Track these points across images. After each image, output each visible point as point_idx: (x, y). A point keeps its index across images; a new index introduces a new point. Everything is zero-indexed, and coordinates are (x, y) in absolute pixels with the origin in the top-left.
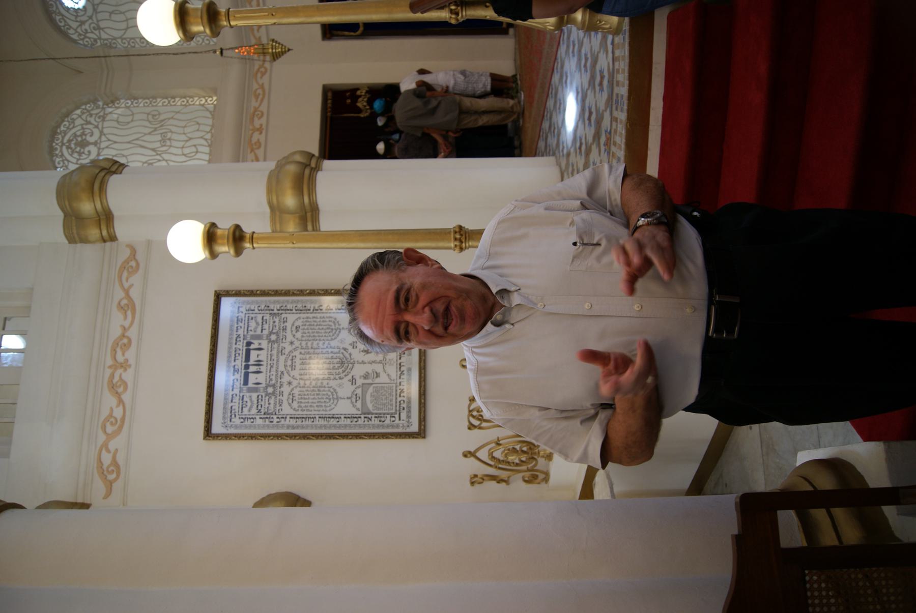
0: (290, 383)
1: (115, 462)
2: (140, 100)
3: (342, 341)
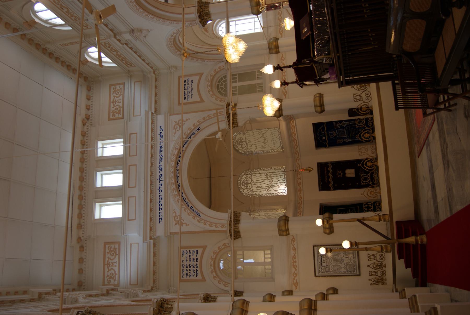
0: (331, 265)
1: (297, 282)
2: (262, 169)
3: (341, 256)
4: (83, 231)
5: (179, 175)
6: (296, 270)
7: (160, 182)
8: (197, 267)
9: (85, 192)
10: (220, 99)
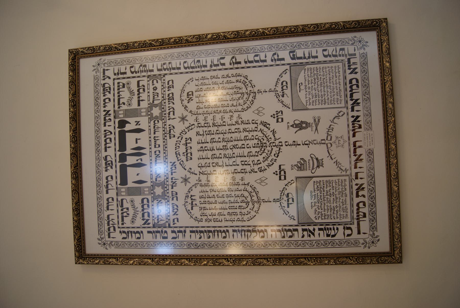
0: (186, 180)
3: (259, 112)
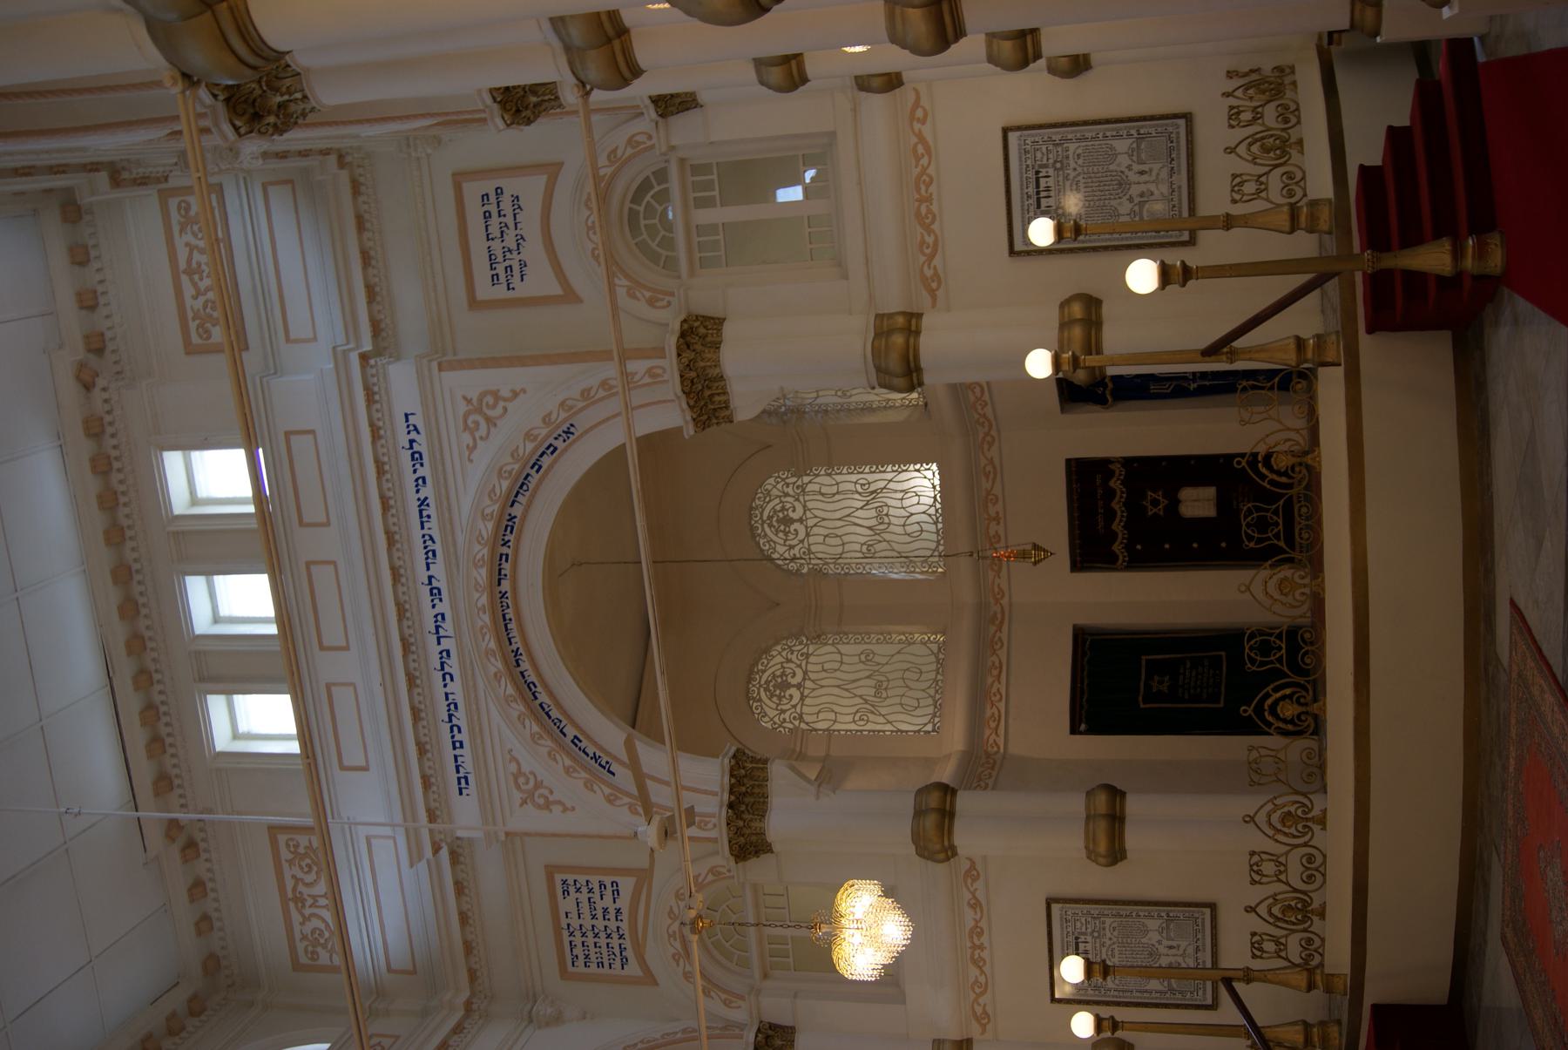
1: (985, 1012)
4: (181, 796)
5: (510, 614)
6: (982, 972)
7: (439, 643)
8: (621, 937)
9: (155, 655)
10: (648, 294)
